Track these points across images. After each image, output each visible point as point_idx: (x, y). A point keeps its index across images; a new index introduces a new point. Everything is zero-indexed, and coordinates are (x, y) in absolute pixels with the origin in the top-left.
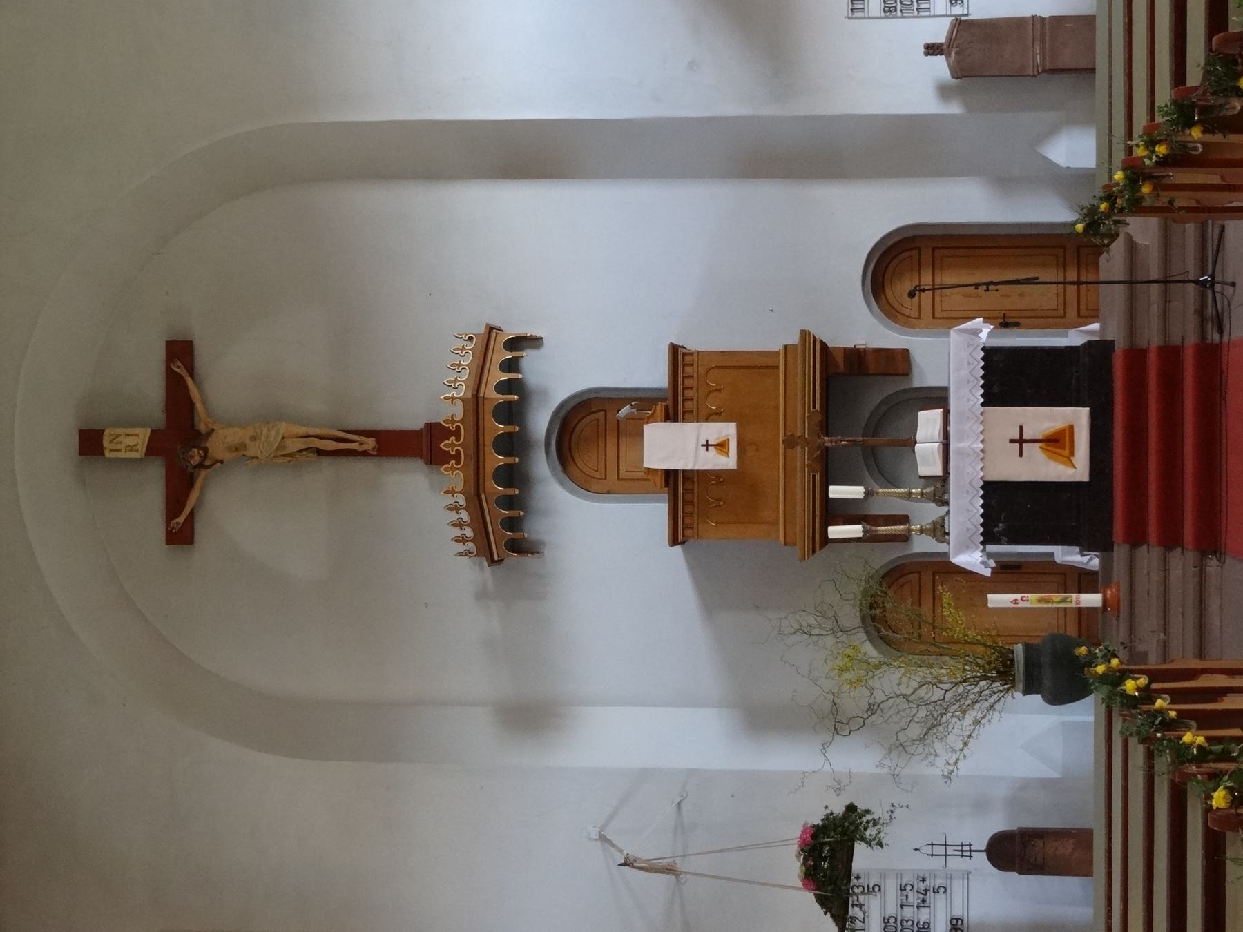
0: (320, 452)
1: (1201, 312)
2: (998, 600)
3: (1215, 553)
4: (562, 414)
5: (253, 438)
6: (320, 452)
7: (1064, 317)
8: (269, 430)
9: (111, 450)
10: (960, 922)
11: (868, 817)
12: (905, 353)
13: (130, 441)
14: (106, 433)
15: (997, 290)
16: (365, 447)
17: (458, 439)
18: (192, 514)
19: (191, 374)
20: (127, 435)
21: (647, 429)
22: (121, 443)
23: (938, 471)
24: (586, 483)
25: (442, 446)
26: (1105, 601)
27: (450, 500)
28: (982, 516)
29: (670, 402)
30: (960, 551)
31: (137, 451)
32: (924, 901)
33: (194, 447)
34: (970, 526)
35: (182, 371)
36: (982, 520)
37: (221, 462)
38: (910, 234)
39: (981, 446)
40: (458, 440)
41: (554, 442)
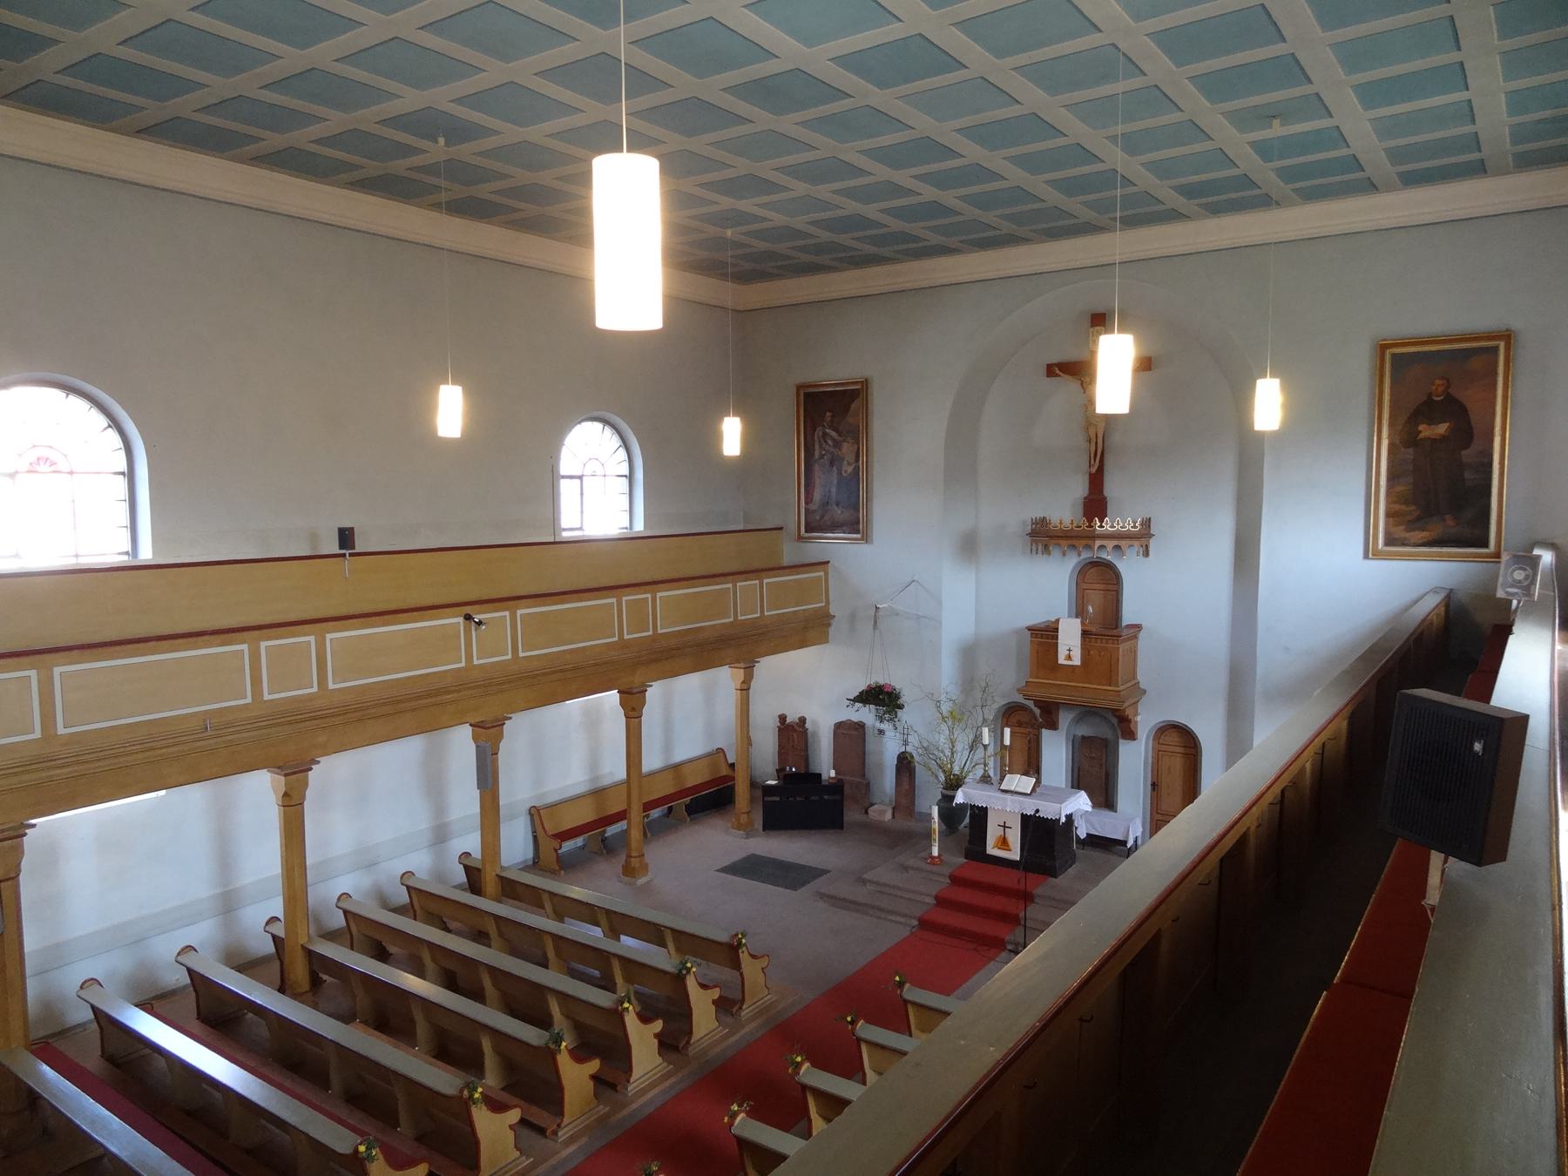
7: (1158, 813)
26: (935, 857)
30: (964, 793)
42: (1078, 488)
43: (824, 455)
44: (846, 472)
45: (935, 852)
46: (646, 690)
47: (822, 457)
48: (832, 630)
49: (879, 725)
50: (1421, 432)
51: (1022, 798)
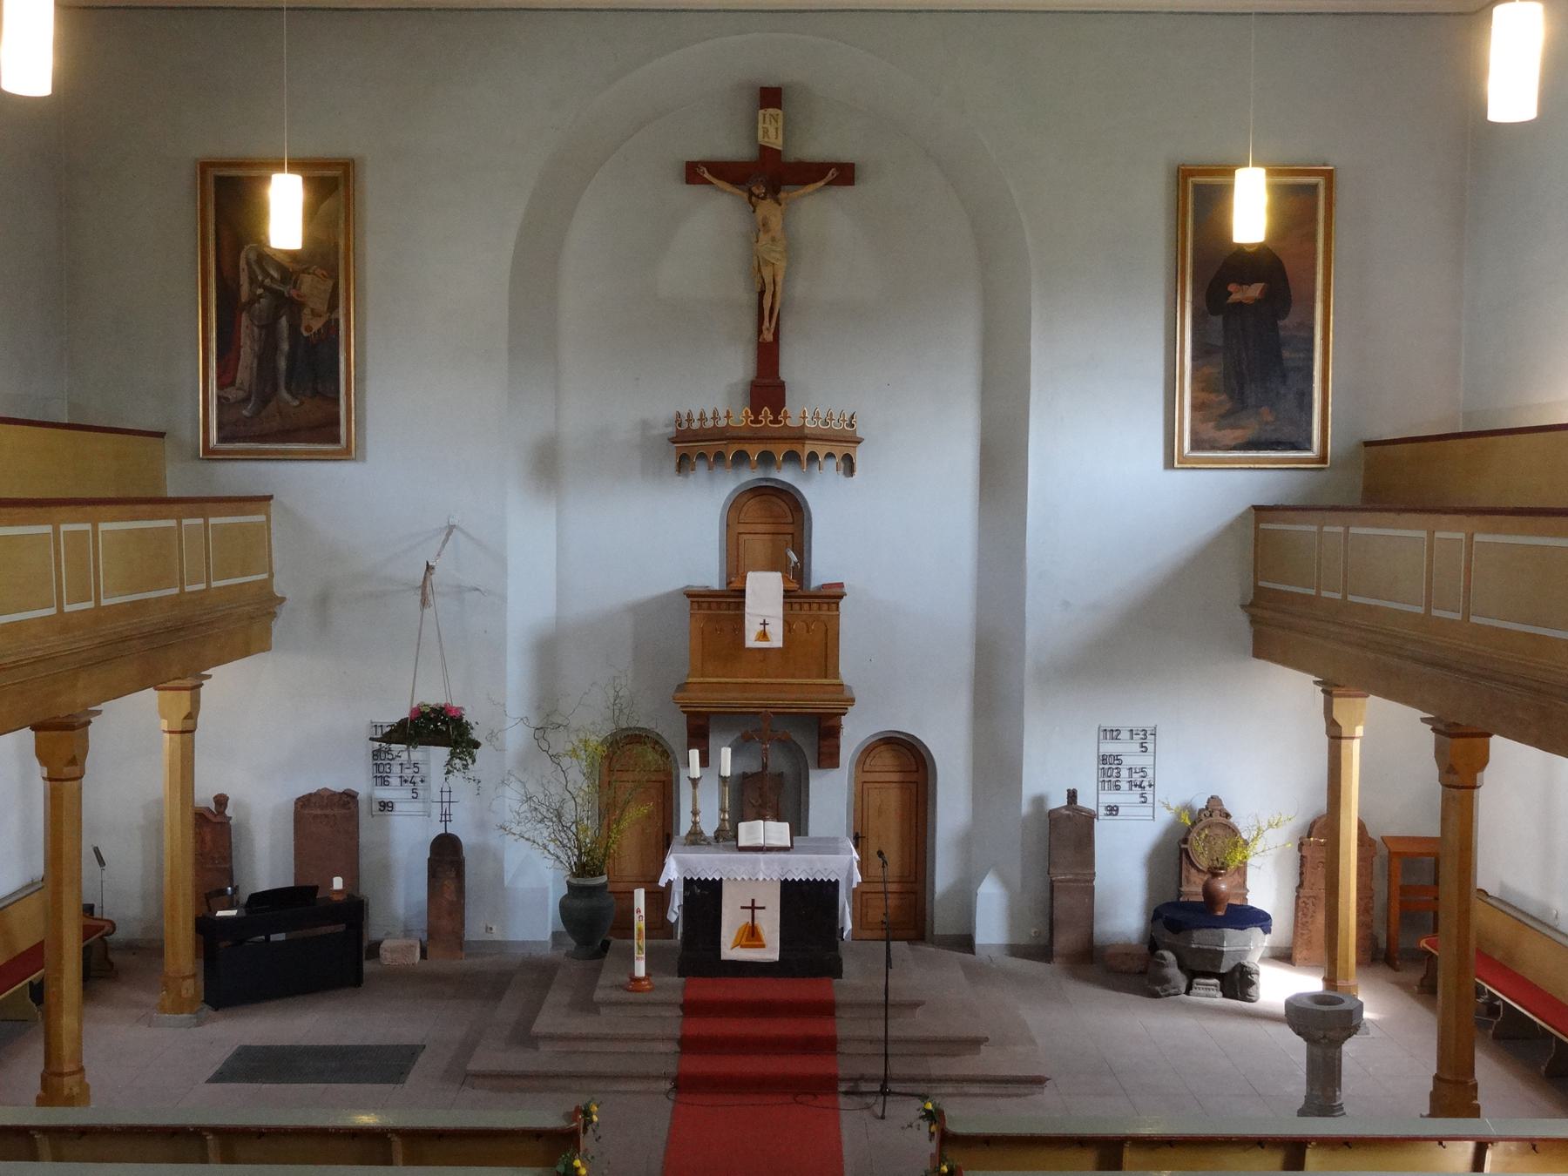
0: (762, 294)
1: (862, 1078)
2: (640, 897)
3: (675, 1087)
4: (791, 491)
5: (773, 240)
6: (762, 294)
10: (390, 809)
11: (470, 761)
12: (836, 765)
13: (772, 131)
14: (779, 111)
15: (880, 854)
16: (765, 332)
17: (771, 422)
18: (710, 183)
20: (777, 129)
21: (779, 575)
22: (771, 124)
23: (742, 842)
24: (735, 509)
25: (766, 408)
26: (639, 980)
27: (722, 413)
28: (706, 879)
29: (800, 592)
30: (680, 862)
31: (764, 138)
32: (406, 781)
34: (699, 869)
35: (830, 176)
36: (703, 879)
37: (754, 212)
38: (929, 768)
39: (761, 879)
40: (771, 422)
41: (769, 484)
42: (738, 367)
43: (260, 296)
44: (309, 328)
45: (640, 969)
46: (89, 722)
47: (254, 299)
48: (277, 627)
49: (383, 794)
50: (1231, 294)
51: (783, 856)
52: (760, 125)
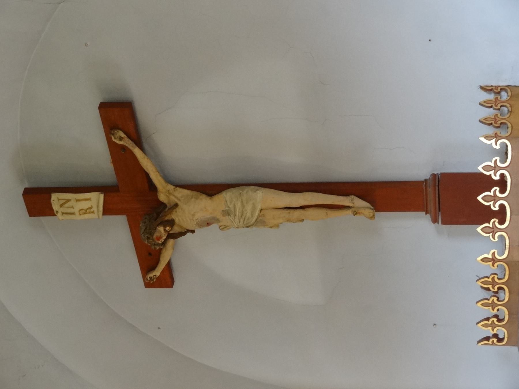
8: (243, 206)
9: (63, 213)
13: (85, 205)
19: (139, 144)
20: (77, 200)
22: (72, 207)
31: (93, 212)
33: (159, 225)
52: (77, 217)
